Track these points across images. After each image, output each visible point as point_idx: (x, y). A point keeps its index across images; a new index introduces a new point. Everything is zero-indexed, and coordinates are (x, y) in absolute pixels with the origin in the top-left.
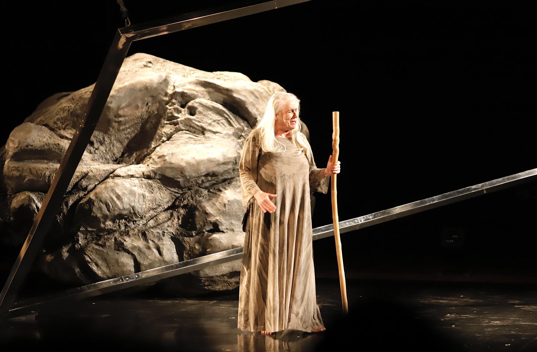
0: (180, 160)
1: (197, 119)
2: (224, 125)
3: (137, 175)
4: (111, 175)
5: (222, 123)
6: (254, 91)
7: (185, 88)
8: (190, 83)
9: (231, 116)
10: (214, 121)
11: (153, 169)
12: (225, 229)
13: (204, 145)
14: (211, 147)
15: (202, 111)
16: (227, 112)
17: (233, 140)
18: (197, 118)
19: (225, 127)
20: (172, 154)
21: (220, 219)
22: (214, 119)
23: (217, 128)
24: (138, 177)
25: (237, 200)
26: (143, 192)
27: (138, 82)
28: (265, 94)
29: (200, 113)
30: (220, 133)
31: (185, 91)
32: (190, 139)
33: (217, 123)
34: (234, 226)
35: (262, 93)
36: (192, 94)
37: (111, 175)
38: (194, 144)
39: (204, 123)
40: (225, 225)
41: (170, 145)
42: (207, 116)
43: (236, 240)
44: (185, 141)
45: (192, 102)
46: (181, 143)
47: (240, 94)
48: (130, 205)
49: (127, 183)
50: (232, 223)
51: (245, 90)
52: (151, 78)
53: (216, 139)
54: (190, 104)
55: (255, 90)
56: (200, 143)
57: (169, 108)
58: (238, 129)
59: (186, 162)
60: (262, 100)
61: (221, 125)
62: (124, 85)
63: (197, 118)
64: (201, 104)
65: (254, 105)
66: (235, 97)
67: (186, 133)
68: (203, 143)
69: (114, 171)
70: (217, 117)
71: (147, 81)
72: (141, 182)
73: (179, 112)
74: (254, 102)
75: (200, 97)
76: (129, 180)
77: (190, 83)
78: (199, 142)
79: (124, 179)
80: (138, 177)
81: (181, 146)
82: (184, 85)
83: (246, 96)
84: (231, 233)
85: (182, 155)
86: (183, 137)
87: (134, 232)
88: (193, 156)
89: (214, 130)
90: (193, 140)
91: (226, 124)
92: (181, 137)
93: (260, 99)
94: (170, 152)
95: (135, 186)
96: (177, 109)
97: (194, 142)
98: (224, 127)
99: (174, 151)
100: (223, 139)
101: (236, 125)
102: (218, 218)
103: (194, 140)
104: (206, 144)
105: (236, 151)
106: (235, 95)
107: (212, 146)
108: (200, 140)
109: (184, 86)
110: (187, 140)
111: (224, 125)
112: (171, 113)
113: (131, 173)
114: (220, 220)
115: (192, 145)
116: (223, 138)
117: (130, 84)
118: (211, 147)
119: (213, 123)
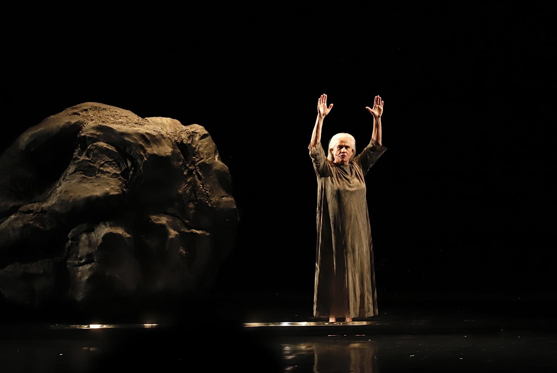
6: (145, 134)
10: (106, 162)
17: (120, 179)
28: (158, 137)
35: (154, 136)
51: (136, 133)
53: (104, 178)
55: (147, 133)
60: (154, 142)
66: (125, 140)
68: (93, 182)
69: (20, 206)
74: (143, 144)
80: (36, 213)
83: (136, 139)
89: (105, 170)
97: (86, 181)
105: (121, 189)
107: (99, 185)
115: (84, 184)
119: (106, 165)
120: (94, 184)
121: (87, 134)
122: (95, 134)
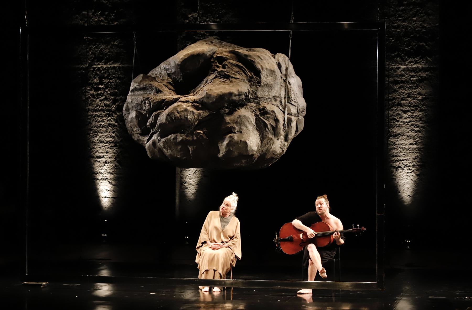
0: (214, 93)
1: (226, 71)
2: (242, 74)
3: (191, 101)
4: (176, 100)
5: (241, 73)
7: (223, 54)
8: (225, 52)
9: (246, 70)
11: (200, 98)
12: (236, 131)
13: (229, 85)
14: (233, 86)
15: (229, 66)
16: (244, 67)
18: (227, 70)
19: (243, 75)
20: (211, 89)
21: (234, 126)
22: (237, 71)
23: (238, 76)
24: (191, 102)
25: (245, 115)
26: (193, 110)
27: (196, 51)
29: (229, 67)
30: (239, 79)
31: (222, 56)
32: (222, 82)
33: (238, 73)
34: (242, 129)
36: (226, 58)
37: (176, 100)
38: (223, 85)
39: (230, 73)
40: (237, 129)
41: (210, 85)
42: (233, 70)
43: (243, 138)
44: (219, 83)
45: (225, 62)
46: (216, 84)
47: (252, 58)
48: (185, 117)
49: (185, 106)
50: (241, 128)
51: (255, 55)
52: (203, 48)
53: (236, 82)
54: (224, 63)
56: (227, 84)
57: (214, 65)
58: (250, 77)
59: (217, 94)
61: (240, 74)
62: (188, 53)
63: (227, 70)
64: (230, 63)
65: (259, 63)
67: (220, 79)
69: (180, 98)
70: (238, 70)
71: (201, 50)
72: (193, 105)
73: (218, 67)
75: (230, 59)
76: (186, 103)
77: (225, 52)
78: (227, 83)
79: (183, 103)
80: (191, 102)
81: (216, 85)
82: (222, 53)
84: (239, 134)
85: (216, 90)
86: (219, 80)
87: (188, 132)
88: (221, 91)
90: (223, 82)
91: (243, 74)
92: (217, 81)
93: (264, 60)
94: (209, 89)
95: (189, 107)
96: (218, 65)
97: (224, 83)
98: (242, 75)
99: (212, 88)
100: (240, 82)
101: (249, 74)
102: (232, 125)
103: (224, 83)
104: (230, 84)
106: (249, 58)
108: (227, 83)
109: (222, 54)
110: (220, 82)
111: (242, 74)
112: (214, 67)
113: (187, 100)
114: (234, 126)
115: (222, 85)
116: (240, 81)
117: (192, 52)
118: (233, 86)
119: (236, 73)
120: (230, 85)
121: (222, 55)
122: (228, 56)
